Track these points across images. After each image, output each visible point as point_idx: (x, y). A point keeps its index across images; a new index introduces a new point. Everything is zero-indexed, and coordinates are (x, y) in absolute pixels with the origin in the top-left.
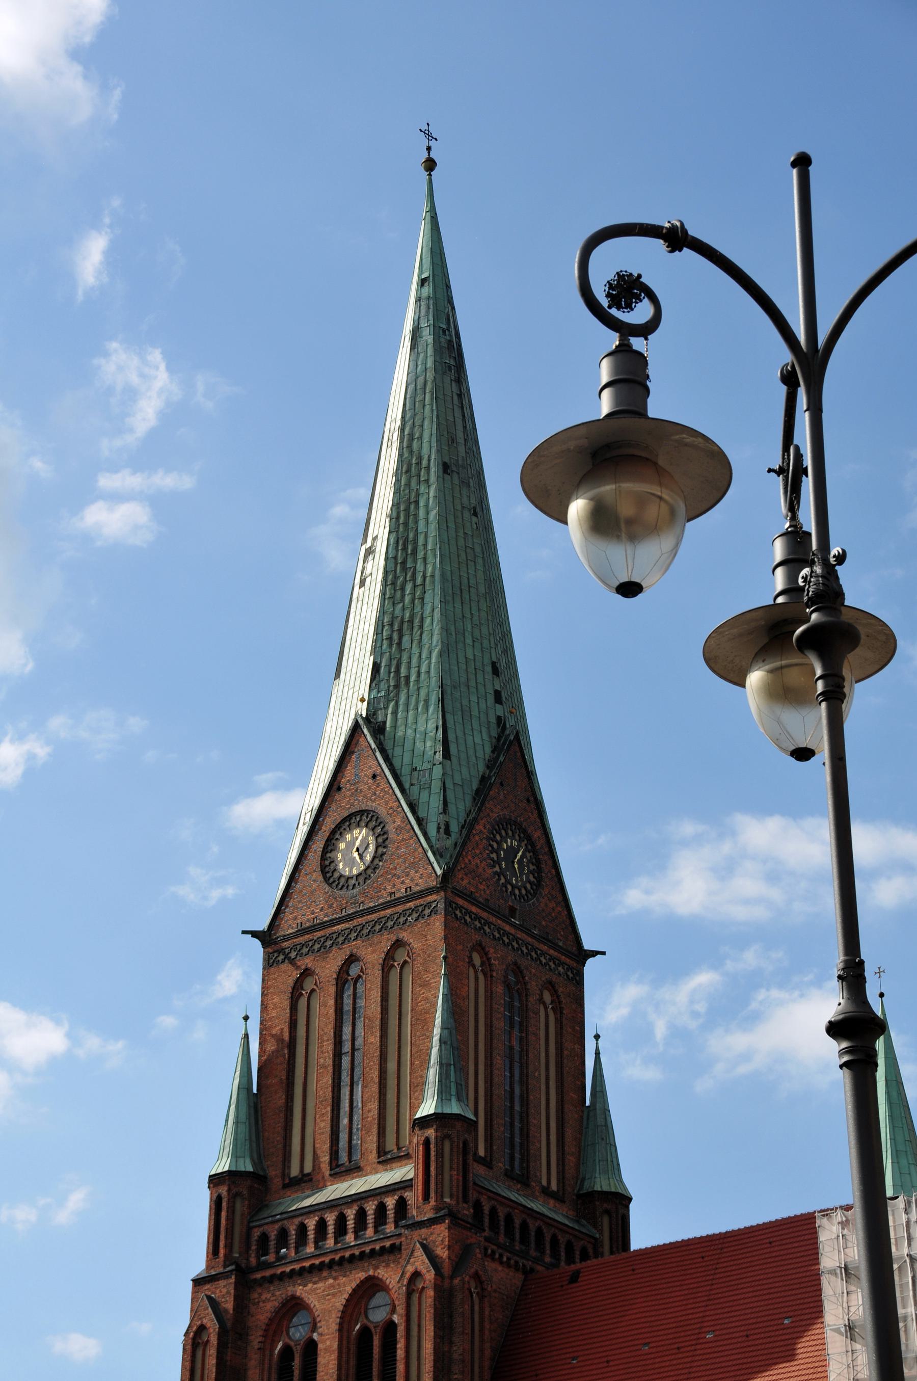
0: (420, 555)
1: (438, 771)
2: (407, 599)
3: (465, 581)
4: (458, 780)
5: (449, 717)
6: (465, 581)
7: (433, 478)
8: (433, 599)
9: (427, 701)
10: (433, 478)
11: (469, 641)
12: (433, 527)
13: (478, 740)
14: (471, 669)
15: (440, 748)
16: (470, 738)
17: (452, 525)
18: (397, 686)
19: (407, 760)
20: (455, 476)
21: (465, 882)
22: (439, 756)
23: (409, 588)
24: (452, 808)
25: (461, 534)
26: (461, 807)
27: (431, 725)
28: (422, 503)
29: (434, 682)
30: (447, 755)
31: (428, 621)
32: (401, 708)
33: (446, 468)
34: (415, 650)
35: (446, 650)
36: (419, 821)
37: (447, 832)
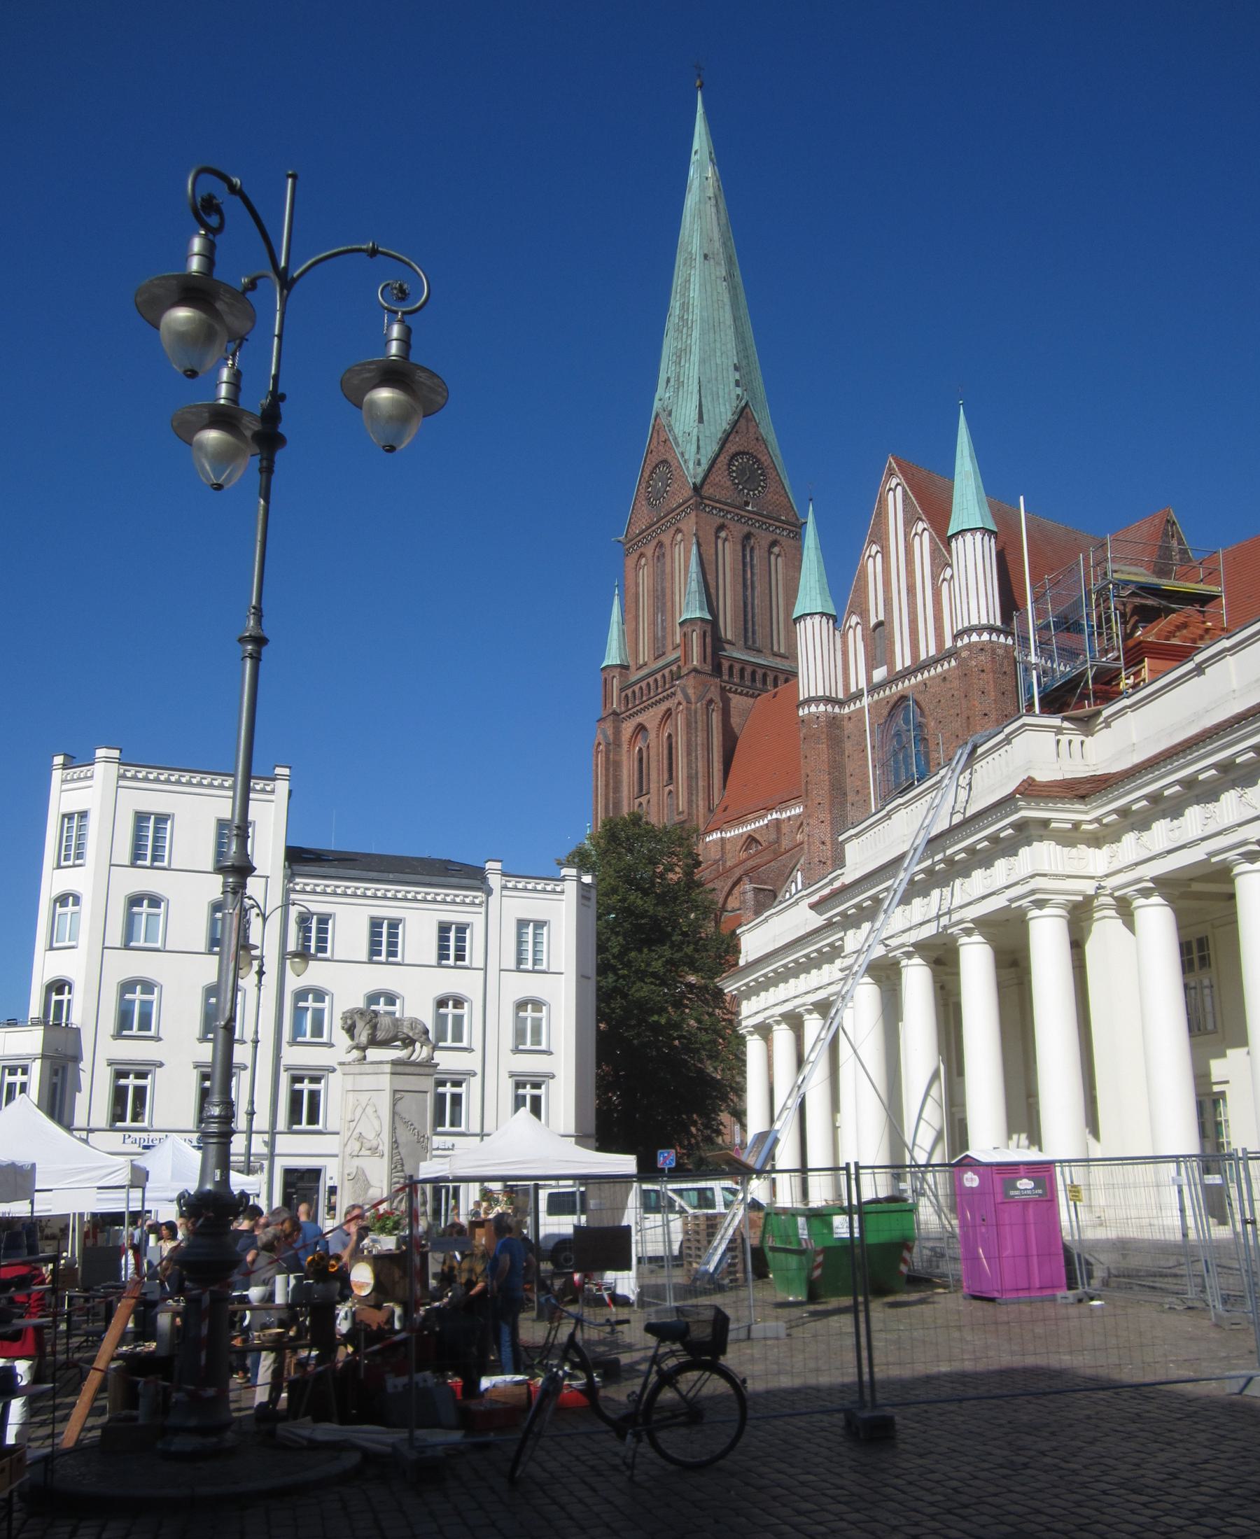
0: (691, 310)
1: (696, 429)
2: (684, 336)
3: (716, 320)
4: (708, 434)
5: (703, 399)
6: (716, 320)
7: (697, 266)
8: (696, 334)
9: (692, 393)
10: (697, 266)
11: (718, 354)
12: (697, 292)
13: (723, 410)
14: (720, 369)
15: (697, 416)
16: (717, 411)
17: (709, 289)
18: (678, 388)
19: (681, 428)
20: (712, 260)
21: (711, 490)
22: (696, 423)
23: (685, 331)
24: (702, 451)
25: (715, 293)
26: (710, 449)
27: (694, 407)
28: (692, 280)
29: (696, 381)
30: (701, 420)
31: (693, 348)
32: (680, 400)
33: (706, 257)
34: (687, 365)
35: (702, 361)
36: (685, 461)
37: (699, 464)
